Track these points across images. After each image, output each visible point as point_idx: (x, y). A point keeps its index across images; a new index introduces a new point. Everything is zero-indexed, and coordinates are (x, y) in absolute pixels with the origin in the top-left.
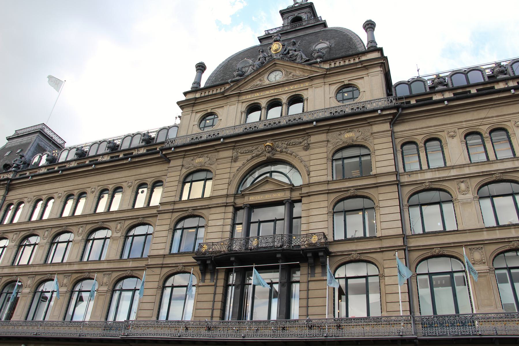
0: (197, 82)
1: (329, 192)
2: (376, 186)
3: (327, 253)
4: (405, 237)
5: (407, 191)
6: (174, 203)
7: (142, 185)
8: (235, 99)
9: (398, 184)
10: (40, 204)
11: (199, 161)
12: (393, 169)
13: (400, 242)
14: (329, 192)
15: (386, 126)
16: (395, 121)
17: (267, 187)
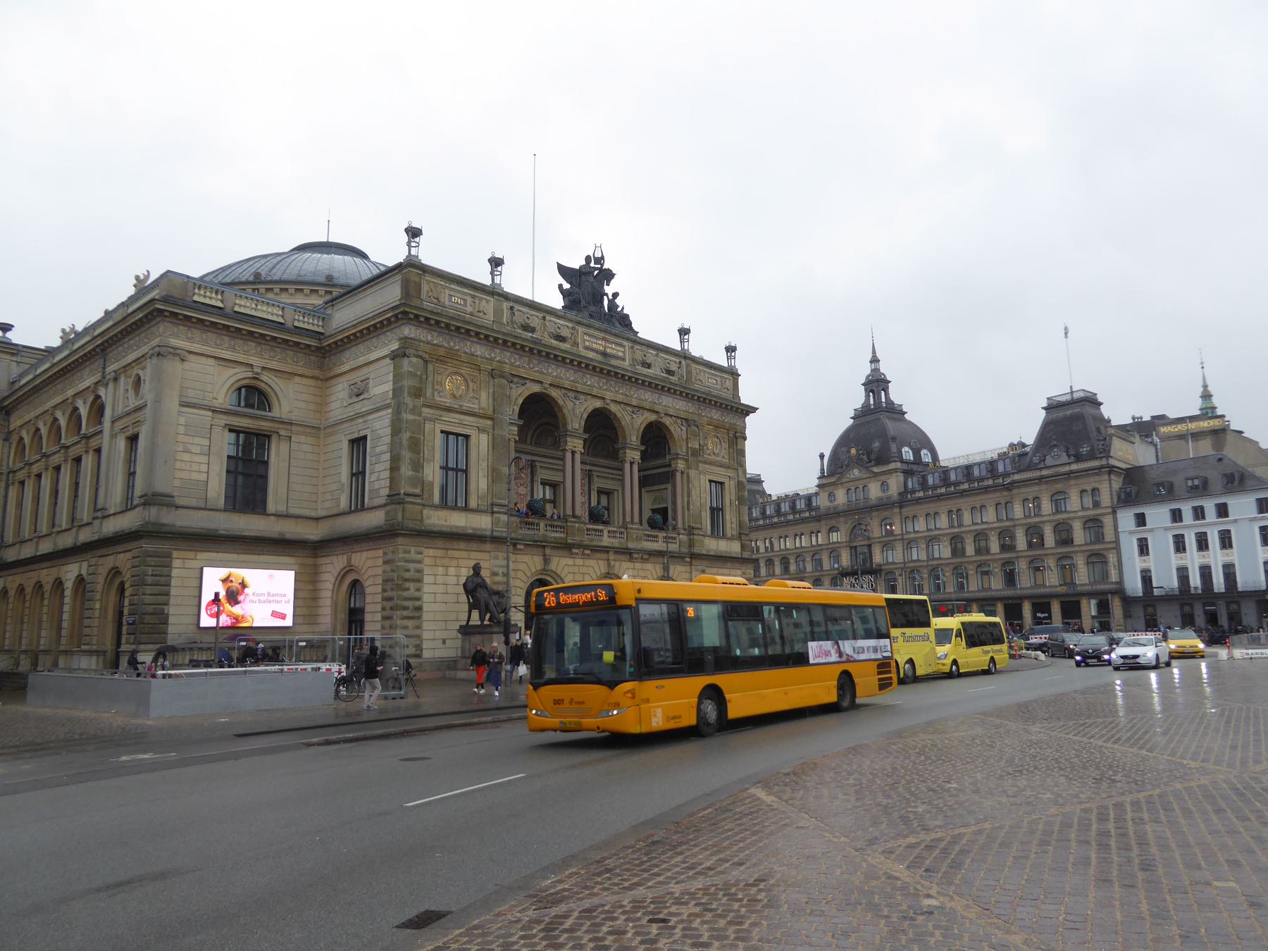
0: (822, 469)
1: (880, 542)
2: (895, 540)
3: (881, 570)
4: (904, 563)
5: (906, 542)
6: (827, 545)
7: (812, 533)
8: (840, 486)
9: (903, 539)
10: (767, 541)
11: (833, 523)
12: (900, 532)
13: (902, 565)
14: (880, 542)
15: (898, 510)
16: (901, 507)
17: (860, 538)
